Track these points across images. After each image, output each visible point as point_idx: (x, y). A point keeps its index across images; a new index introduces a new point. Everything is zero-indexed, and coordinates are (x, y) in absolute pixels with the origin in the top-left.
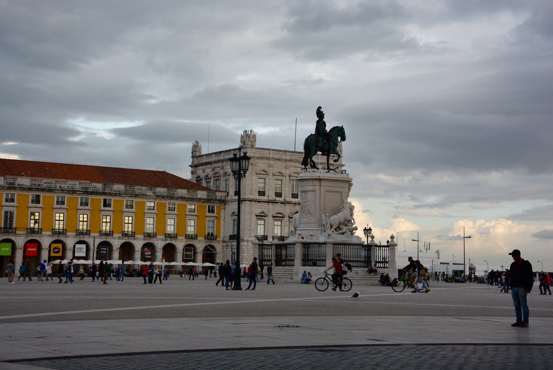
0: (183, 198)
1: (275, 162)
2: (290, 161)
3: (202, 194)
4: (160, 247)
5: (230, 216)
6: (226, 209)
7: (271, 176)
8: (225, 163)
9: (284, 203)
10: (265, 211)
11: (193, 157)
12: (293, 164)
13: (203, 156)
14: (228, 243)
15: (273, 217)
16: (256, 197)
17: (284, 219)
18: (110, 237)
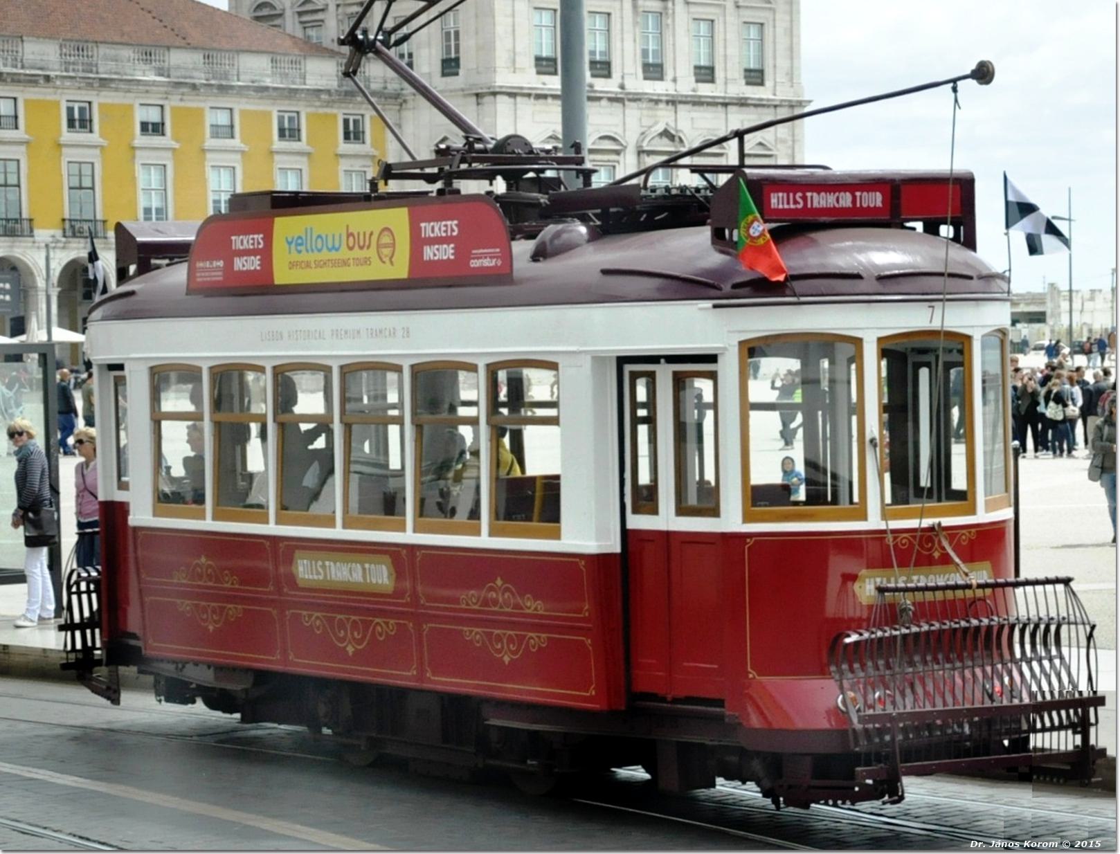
17: (621, 158)
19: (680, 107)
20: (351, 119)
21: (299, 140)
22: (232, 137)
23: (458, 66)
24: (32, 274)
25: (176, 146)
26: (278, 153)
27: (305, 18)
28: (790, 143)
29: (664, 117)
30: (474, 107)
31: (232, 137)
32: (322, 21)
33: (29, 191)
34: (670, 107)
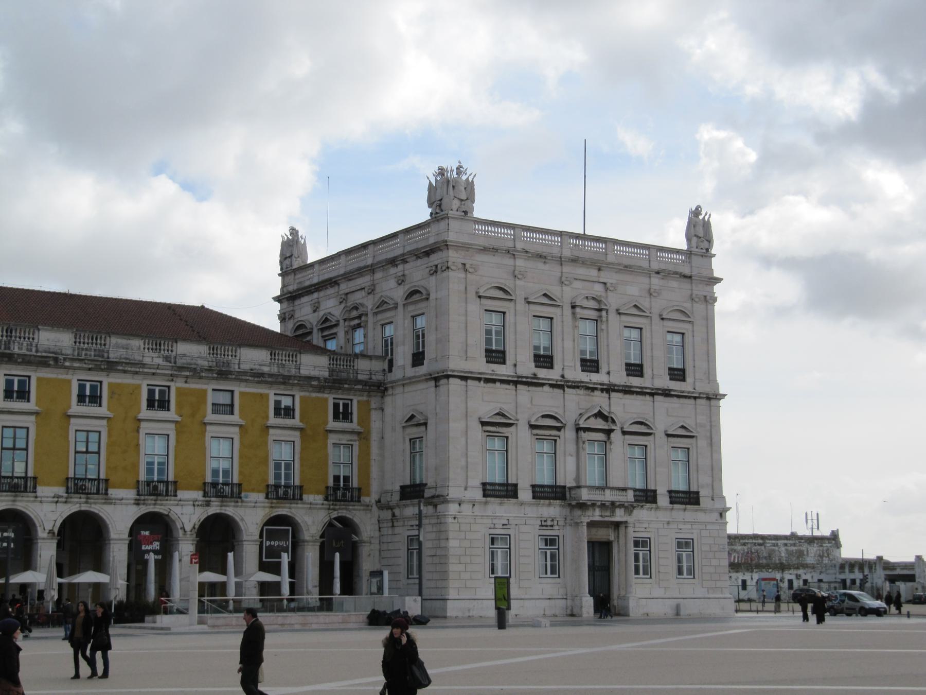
0: (258, 377)
1: (531, 264)
2: (574, 260)
3: (313, 365)
4: (188, 527)
5: (399, 428)
6: (388, 410)
7: (521, 306)
8: (379, 275)
9: (560, 385)
10: (509, 409)
11: (284, 274)
12: (581, 271)
13: (312, 265)
14: (397, 511)
15: (532, 427)
16: (480, 365)
17: (561, 434)
18: (29, 497)
19: (613, 394)
20: (341, 402)
21: (294, 418)
22: (232, 413)
23: (424, 358)
24: (34, 525)
25: (179, 419)
26: (273, 427)
27: (326, 333)
28: (708, 427)
29: (599, 401)
30: (433, 389)
31: (232, 413)
32: (335, 334)
33: (36, 454)
34: (605, 395)
